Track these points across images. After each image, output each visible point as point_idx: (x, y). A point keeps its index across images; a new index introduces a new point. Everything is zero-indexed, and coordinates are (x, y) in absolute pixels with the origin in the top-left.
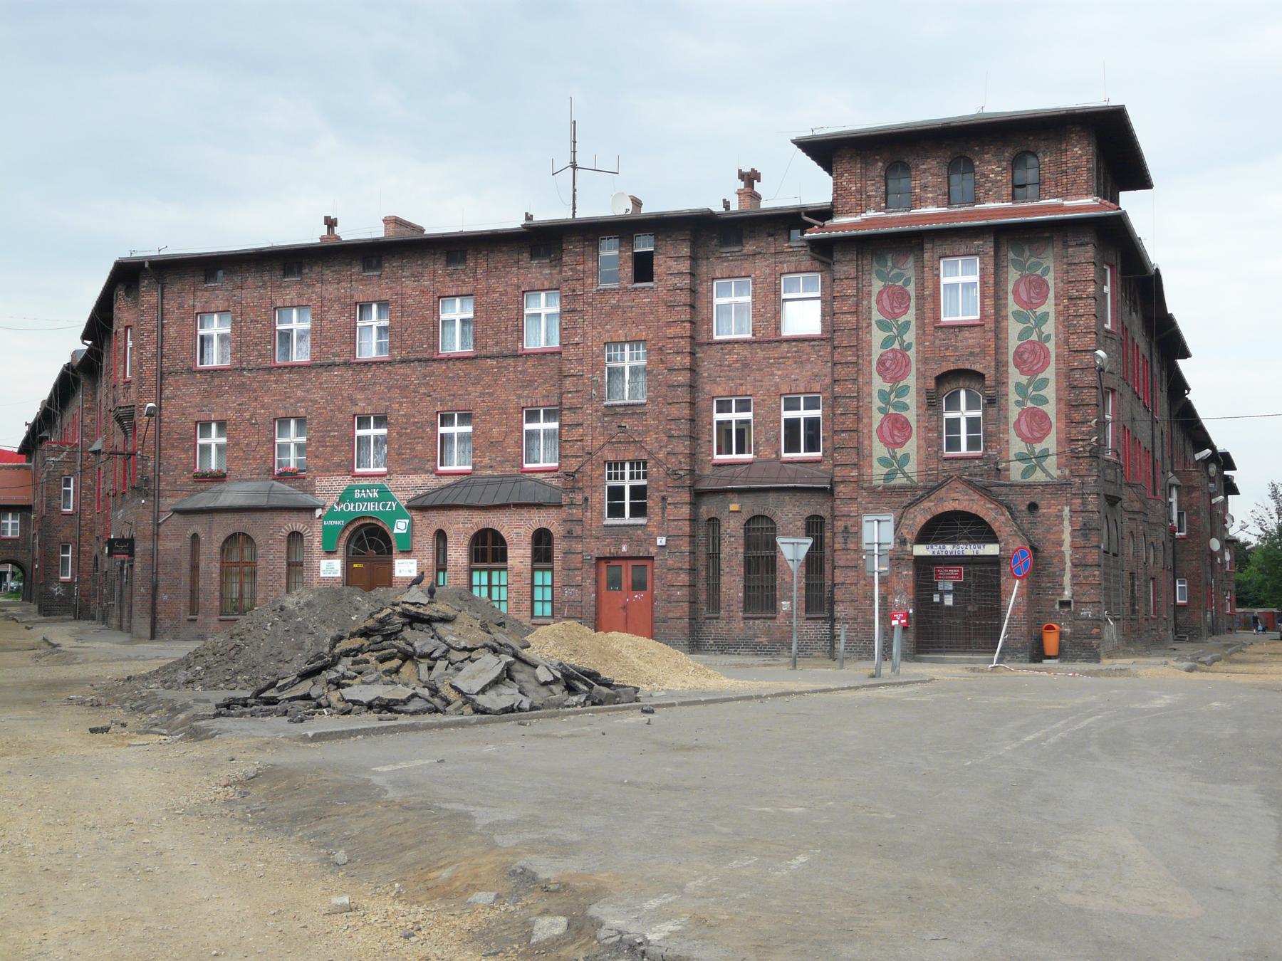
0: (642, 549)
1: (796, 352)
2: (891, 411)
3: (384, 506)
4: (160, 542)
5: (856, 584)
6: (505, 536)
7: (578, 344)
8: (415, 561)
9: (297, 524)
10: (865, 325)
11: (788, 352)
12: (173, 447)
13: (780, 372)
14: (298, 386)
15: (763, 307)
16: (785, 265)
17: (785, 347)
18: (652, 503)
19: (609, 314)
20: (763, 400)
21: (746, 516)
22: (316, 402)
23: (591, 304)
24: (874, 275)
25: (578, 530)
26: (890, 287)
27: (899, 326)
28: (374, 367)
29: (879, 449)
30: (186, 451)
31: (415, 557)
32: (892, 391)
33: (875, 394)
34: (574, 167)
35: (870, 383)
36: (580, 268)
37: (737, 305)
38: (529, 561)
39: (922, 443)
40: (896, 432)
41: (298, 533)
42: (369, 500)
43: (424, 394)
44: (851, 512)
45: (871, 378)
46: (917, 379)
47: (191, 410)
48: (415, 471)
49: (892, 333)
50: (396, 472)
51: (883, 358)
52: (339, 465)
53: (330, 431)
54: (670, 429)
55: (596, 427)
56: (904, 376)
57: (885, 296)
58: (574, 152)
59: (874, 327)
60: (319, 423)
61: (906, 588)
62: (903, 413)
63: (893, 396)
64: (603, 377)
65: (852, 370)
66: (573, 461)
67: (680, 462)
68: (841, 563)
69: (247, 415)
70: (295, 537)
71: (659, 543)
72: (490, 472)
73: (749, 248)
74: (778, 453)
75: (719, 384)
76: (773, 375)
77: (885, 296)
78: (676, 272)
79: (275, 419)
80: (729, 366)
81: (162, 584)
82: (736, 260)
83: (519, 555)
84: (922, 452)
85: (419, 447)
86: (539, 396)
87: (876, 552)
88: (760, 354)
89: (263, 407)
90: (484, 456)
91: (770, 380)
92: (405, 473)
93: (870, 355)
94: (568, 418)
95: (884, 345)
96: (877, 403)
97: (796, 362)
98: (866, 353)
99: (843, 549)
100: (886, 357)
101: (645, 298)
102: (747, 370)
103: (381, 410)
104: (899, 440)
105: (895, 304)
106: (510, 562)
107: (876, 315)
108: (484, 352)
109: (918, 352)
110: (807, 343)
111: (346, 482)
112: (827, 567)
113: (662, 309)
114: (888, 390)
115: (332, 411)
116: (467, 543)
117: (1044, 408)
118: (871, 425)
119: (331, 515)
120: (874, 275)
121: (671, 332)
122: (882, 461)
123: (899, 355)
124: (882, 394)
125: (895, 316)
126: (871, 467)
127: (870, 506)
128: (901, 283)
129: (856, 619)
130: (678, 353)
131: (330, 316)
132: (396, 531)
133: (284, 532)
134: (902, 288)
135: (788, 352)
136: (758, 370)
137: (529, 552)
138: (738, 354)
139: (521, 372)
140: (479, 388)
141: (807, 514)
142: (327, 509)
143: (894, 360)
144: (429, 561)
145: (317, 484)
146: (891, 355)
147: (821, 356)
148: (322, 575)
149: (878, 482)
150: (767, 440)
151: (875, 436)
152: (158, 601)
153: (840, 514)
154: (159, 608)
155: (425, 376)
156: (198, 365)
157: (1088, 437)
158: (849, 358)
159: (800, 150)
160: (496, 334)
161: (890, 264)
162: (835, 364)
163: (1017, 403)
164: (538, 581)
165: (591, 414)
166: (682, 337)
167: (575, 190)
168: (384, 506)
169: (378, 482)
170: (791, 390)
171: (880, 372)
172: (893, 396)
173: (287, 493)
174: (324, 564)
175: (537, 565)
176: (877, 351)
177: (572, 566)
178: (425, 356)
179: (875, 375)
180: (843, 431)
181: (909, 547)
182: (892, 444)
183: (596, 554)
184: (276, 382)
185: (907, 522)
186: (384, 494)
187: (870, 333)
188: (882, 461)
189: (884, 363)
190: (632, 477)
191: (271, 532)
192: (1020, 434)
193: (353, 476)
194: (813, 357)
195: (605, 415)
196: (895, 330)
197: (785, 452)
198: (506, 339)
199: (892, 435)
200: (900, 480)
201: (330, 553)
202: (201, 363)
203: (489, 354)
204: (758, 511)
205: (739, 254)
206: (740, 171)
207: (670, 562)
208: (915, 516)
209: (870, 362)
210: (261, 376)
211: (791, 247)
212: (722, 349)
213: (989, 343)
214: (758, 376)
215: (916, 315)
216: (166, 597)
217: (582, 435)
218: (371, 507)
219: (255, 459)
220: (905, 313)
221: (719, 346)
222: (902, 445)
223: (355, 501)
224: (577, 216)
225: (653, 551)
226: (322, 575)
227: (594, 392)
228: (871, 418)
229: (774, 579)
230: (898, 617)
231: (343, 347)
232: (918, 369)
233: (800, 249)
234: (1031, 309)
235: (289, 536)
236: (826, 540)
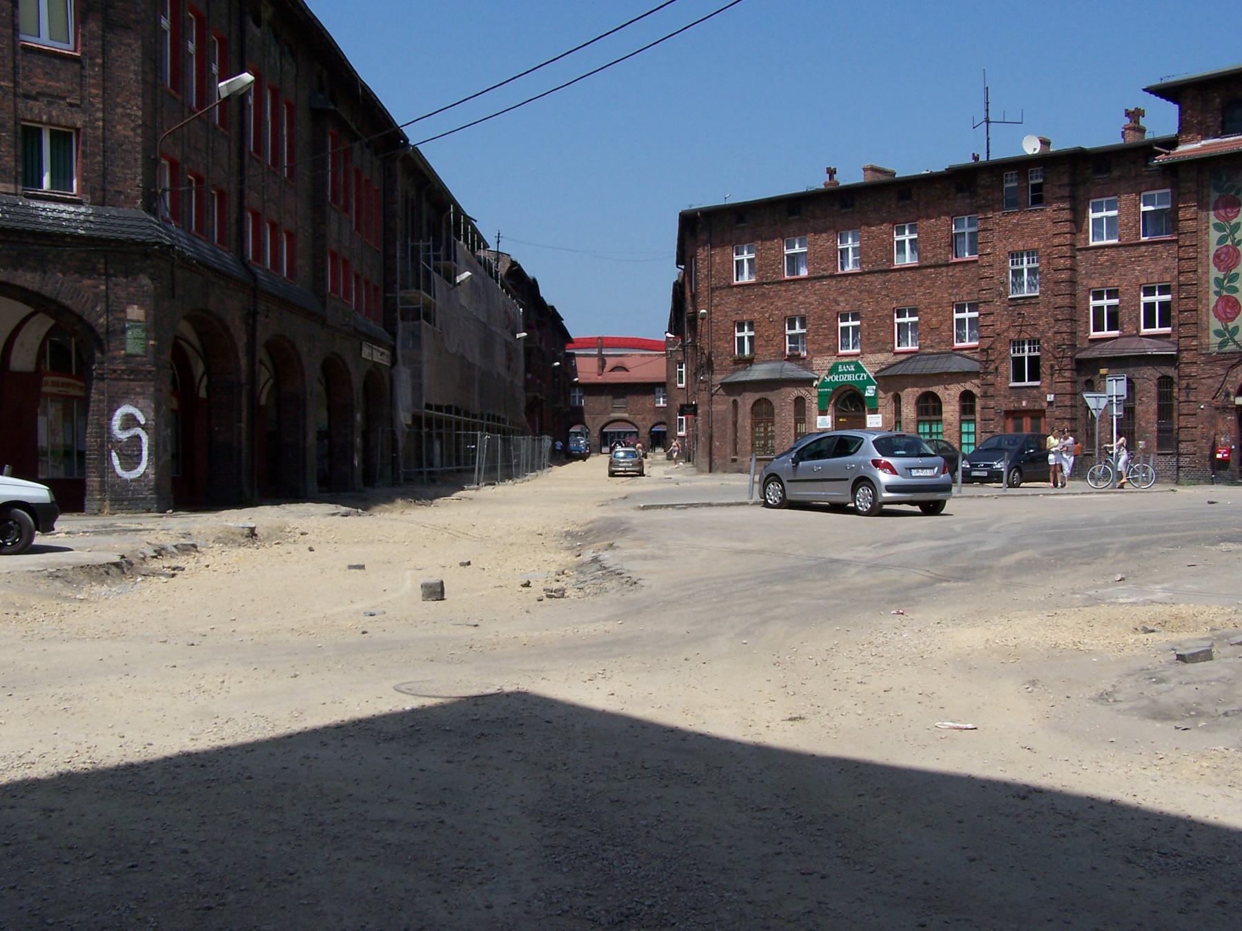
0: (1037, 404)
1: (1152, 251)
2: (1225, 293)
3: (859, 377)
4: (713, 406)
5: (1195, 428)
6: (940, 397)
7: (989, 254)
8: (880, 416)
9: (802, 392)
10: (1204, 228)
12: (720, 340)
14: (800, 293)
15: (1127, 219)
17: (1143, 248)
18: (1044, 369)
19: (1010, 231)
20: (1127, 290)
22: (811, 304)
23: (998, 224)
25: (991, 391)
26: (1223, 196)
27: (1231, 226)
28: (850, 278)
30: (728, 342)
31: (880, 413)
33: (1212, 281)
34: (988, 122)
35: (1207, 273)
36: (990, 197)
37: (1107, 218)
38: (957, 415)
40: (1228, 310)
41: (802, 398)
42: (849, 372)
43: (884, 295)
44: (1192, 372)
45: (1208, 269)
47: (731, 313)
48: (880, 351)
50: (867, 352)
52: (828, 348)
53: (821, 325)
54: (1057, 315)
55: (1003, 315)
58: (987, 110)
59: (1212, 230)
60: (814, 319)
61: (1229, 431)
62: (1233, 295)
63: (1226, 281)
64: (1007, 278)
65: (1193, 263)
66: (987, 340)
67: (1064, 339)
68: (1185, 412)
69: (767, 315)
70: (800, 402)
71: (1048, 400)
72: (931, 350)
73: (1116, 173)
74: (1138, 330)
75: (1094, 279)
76: (1134, 270)
79: (785, 318)
80: (1101, 264)
81: (714, 435)
83: (951, 410)
85: (882, 334)
86: (964, 293)
87: (1115, 401)
88: (1125, 254)
89: (777, 309)
90: (926, 339)
91: (1133, 274)
92: (872, 352)
93: (1207, 251)
94: (983, 309)
97: (1152, 260)
98: (1204, 249)
99: (1185, 402)
101: (1037, 217)
102: (1114, 268)
103: (856, 309)
104: (1230, 316)
106: (944, 415)
108: (925, 263)
111: (834, 359)
112: (1175, 415)
113: (1049, 224)
114: (1222, 277)
115: (822, 310)
116: (914, 402)
118: (1208, 305)
119: (824, 384)
121: (1056, 241)
122: (1218, 333)
123: (1231, 250)
124: (1217, 280)
125: (1228, 219)
126: (1208, 338)
129: (1195, 454)
130: (1061, 257)
131: (820, 242)
132: (867, 395)
133: (793, 397)
137: (957, 408)
138: (1107, 255)
139: (951, 276)
140: (922, 289)
141: (1158, 375)
142: (820, 380)
143: (1227, 254)
144: (891, 416)
145: (814, 362)
148: (818, 427)
150: (1130, 320)
151: (1211, 313)
152: (713, 447)
154: (714, 451)
155: (885, 282)
156: (735, 281)
159: (1153, 96)
160: (933, 249)
162: (1180, 260)
164: (965, 429)
165: (999, 306)
167: (988, 139)
168: (859, 377)
169: (854, 359)
172: (1226, 281)
173: (791, 370)
174: (820, 419)
175: (964, 417)
177: (987, 417)
178: (885, 267)
180: (1186, 311)
181: (1232, 398)
182: (1225, 319)
183: (1004, 408)
184: (785, 291)
185: (1231, 379)
186: (859, 369)
187: (1208, 233)
188: (1218, 333)
190: (1030, 351)
191: (783, 397)
193: (838, 356)
195: (1010, 306)
196: (1228, 231)
197: (1145, 328)
198: (941, 253)
199: (1225, 312)
201: (823, 412)
202: (737, 280)
203: (928, 264)
206: (1126, 110)
207: (1057, 413)
208: (1238, 375)
209: (1208, 256)
210: (775, 288)
214: (1122, 271)
216: (717, 444)
217: (993, 321)
218: (850, 377)
219: (772, 345)
221: (1093, 251)
222: (1233, 319)
223: (839, 374)
224: (990, 159)
225: (1045, 405)
226: (818, 427)
227: (1001, 289)
228: (1208, 299)
229: (1133, 425)
230: (1222, 451)
231: (829, 264)
235: (795, 400)
236: (1175, 395)
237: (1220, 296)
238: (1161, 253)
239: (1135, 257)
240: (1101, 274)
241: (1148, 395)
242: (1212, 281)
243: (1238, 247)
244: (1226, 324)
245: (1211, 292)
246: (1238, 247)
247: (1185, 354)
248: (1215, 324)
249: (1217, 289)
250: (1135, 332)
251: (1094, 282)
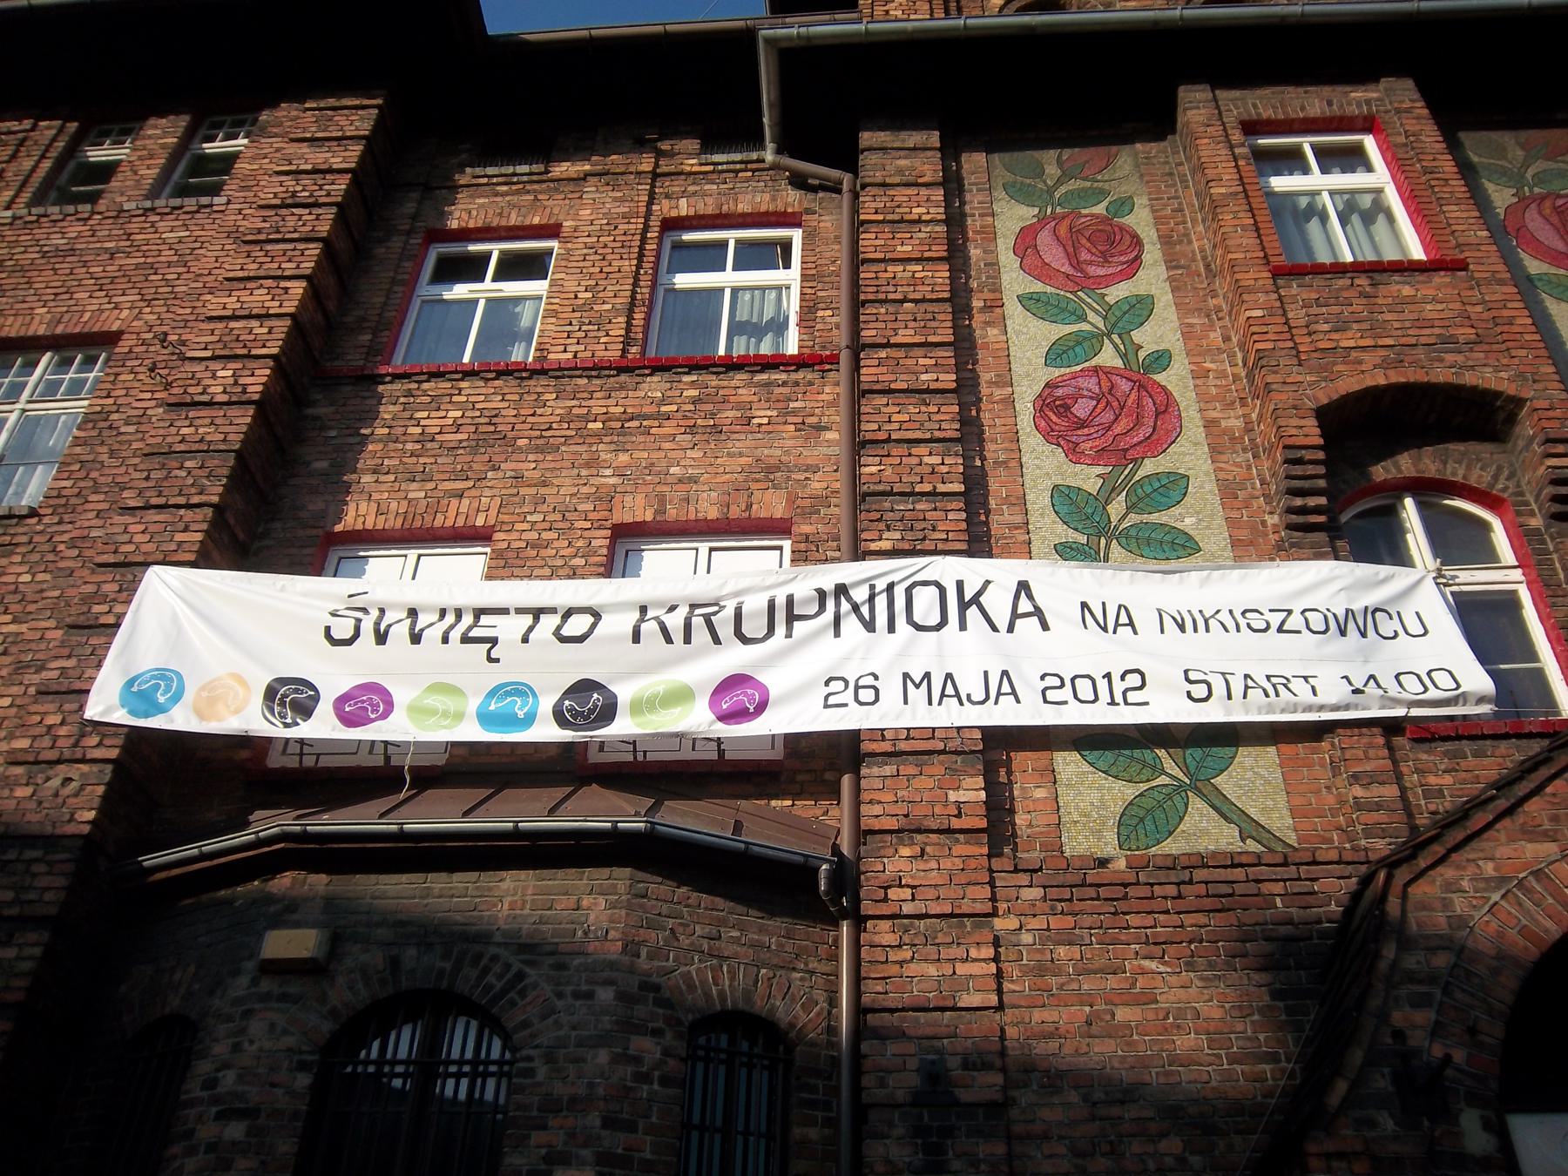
1: (695, 401)
11: (663, 401)
13: (624, 458)
16: (683, 202)
20: (537, 545)
24: (1000, 193)
32: (1109, 492)
33: (1039, 500)
44: (964, 984)
46: (1215, 451)
49: (1085, 327)
51: (1059, 392)
56: (1157, 443)
57: (1044, 238)
59: (1013, 309)
76: (593, 463)
77: (1044, 238)
78: (309, 167)
82: (518, 192)
88: (555, 407)
95: (1057, 353)
97: (692, 429)
100: (1070, 390)
105: (1084, 256)
107: (1015, 281)
109: (1200, 374)
110: (742, 376)
120: (1000, 193)
123: (1124, 386)
127: (1062, 951)
128: (1100, 209)
134: (1105, 220)
135: (663, 401)
136: (539, 450)
146: (1091, 384)
147: (794, 413)
153: (893, 1000)
166: (258, 317)
170: (661, 511)
179: (1032, 442)
189: (1067, 408)
194: (762, 415)
209: (1010, 402)
212: (409, 394)
213: (1506, 313)
215: (1171, 279)
232: (1210, 424)
239: (607, 418)
241: (616, 1142)
243: (1159, 378)
246: (1159, 378)
247: (898, 861)
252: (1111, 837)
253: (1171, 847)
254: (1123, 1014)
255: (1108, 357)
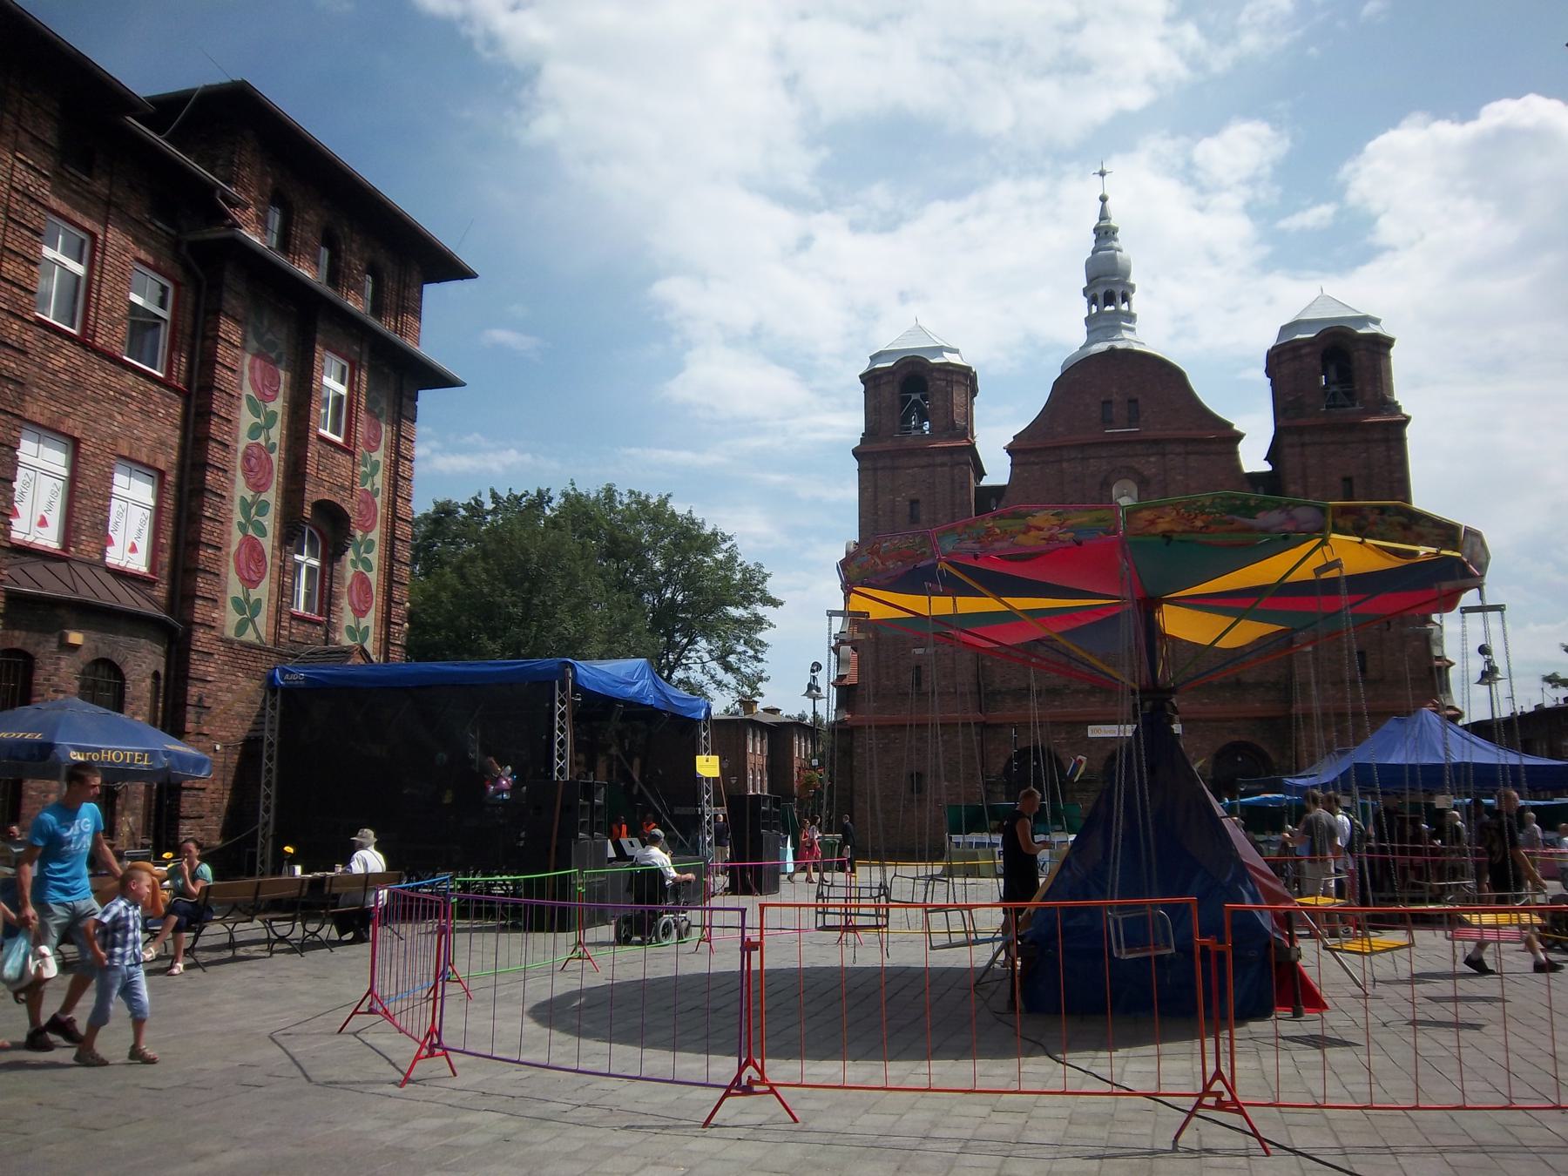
2: (251, 532)
20: (94, 455)
21: (86, 656)
29: (234, 587)
39: (275, 586)
44: (208, 673)
59: (244, 402)
76: (111, 417)
84: (274, 601)
95: (255, 431)
96: (238, 517)
97: (142, 411)
104: (255, 578)
117: (369, 575)
138: (68, 358)
149: (230, 633)
153: (194, 676)
157: (400, 622)
158: (225, 437)
161: (266, 323)
163: (354, 564)
171: (245, 474)
176: (244, 441)
179: (239, 474)
182: (250, 583)
187: (239, 408)
192: (351, 603)
200: (249, 636)
204: (105, 652)
205: (86, 187)
211: (153, 224)
214: (90, 406)
220: (273, 398)
233: (164, 234)
234: (369, 452)
237: (245, 535)
238: (156, 404)
240: (53, 397)
242: (237, 501)
244: (247, 591)
245: (235, 522)
248: (234, 587)
249: (243, 521)
250: (98, 557)
251: (36, 409)
252: (233, 632)
253: (244, 638)
254: (234, 687)
255: (262, 440)
